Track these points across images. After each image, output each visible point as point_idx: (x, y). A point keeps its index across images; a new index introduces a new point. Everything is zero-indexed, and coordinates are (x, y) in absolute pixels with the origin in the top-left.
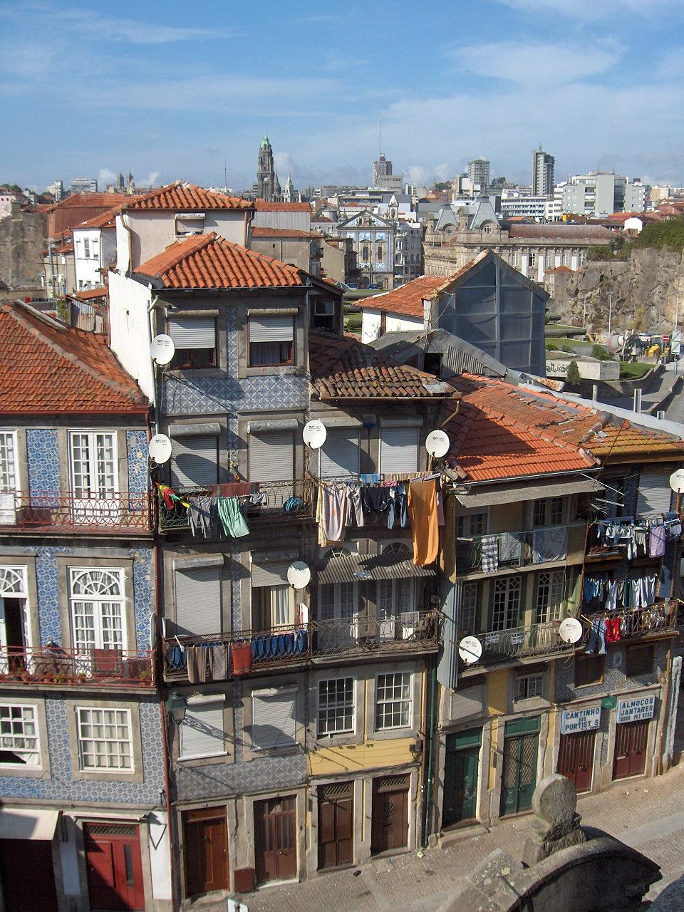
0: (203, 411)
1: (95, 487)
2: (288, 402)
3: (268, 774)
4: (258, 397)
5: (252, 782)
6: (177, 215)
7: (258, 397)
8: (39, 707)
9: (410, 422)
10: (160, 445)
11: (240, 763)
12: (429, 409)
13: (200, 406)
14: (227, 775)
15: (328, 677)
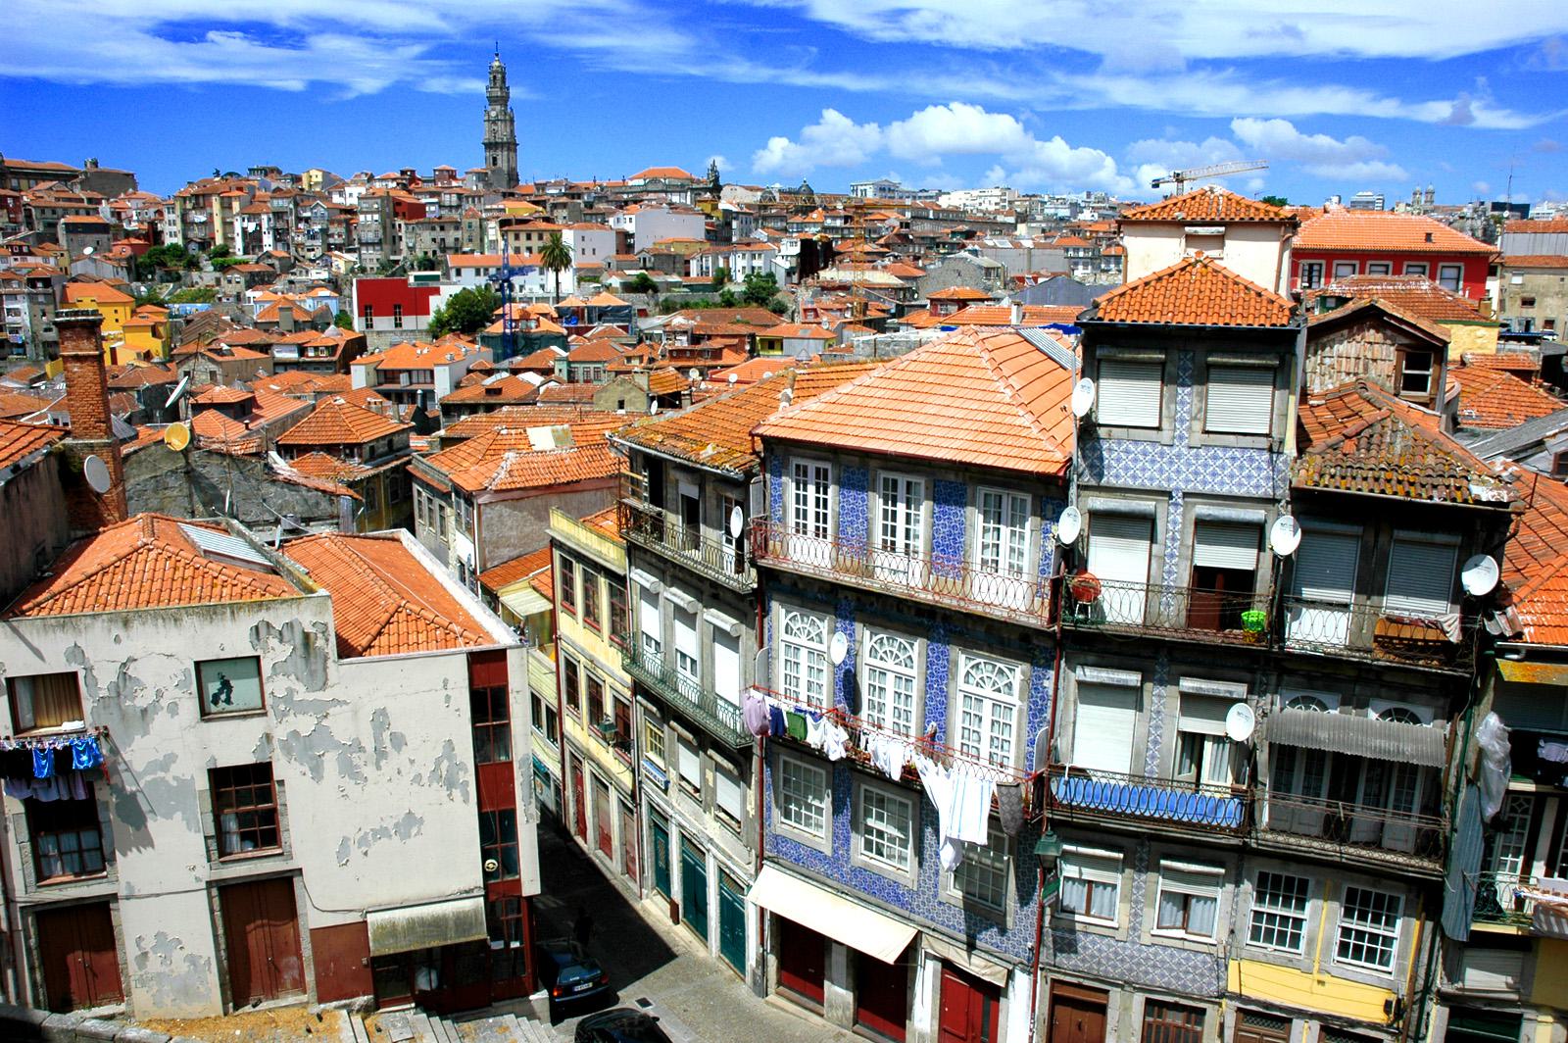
0: (1137, 485)
1: (1004, 561)
2: (1257, 487)
3: (1171, 970)
4: (1214, 474)
5: (1146, 973)
6: (1187, 229)
7: (1214, 474)
8: (914, 804)
9: (1440, 538)
10: (1071, 519)
11: (1134, 943)
12: (1478, 523)
13: (1134, 477)
14: (1116, 953)
15: (1273, 869)
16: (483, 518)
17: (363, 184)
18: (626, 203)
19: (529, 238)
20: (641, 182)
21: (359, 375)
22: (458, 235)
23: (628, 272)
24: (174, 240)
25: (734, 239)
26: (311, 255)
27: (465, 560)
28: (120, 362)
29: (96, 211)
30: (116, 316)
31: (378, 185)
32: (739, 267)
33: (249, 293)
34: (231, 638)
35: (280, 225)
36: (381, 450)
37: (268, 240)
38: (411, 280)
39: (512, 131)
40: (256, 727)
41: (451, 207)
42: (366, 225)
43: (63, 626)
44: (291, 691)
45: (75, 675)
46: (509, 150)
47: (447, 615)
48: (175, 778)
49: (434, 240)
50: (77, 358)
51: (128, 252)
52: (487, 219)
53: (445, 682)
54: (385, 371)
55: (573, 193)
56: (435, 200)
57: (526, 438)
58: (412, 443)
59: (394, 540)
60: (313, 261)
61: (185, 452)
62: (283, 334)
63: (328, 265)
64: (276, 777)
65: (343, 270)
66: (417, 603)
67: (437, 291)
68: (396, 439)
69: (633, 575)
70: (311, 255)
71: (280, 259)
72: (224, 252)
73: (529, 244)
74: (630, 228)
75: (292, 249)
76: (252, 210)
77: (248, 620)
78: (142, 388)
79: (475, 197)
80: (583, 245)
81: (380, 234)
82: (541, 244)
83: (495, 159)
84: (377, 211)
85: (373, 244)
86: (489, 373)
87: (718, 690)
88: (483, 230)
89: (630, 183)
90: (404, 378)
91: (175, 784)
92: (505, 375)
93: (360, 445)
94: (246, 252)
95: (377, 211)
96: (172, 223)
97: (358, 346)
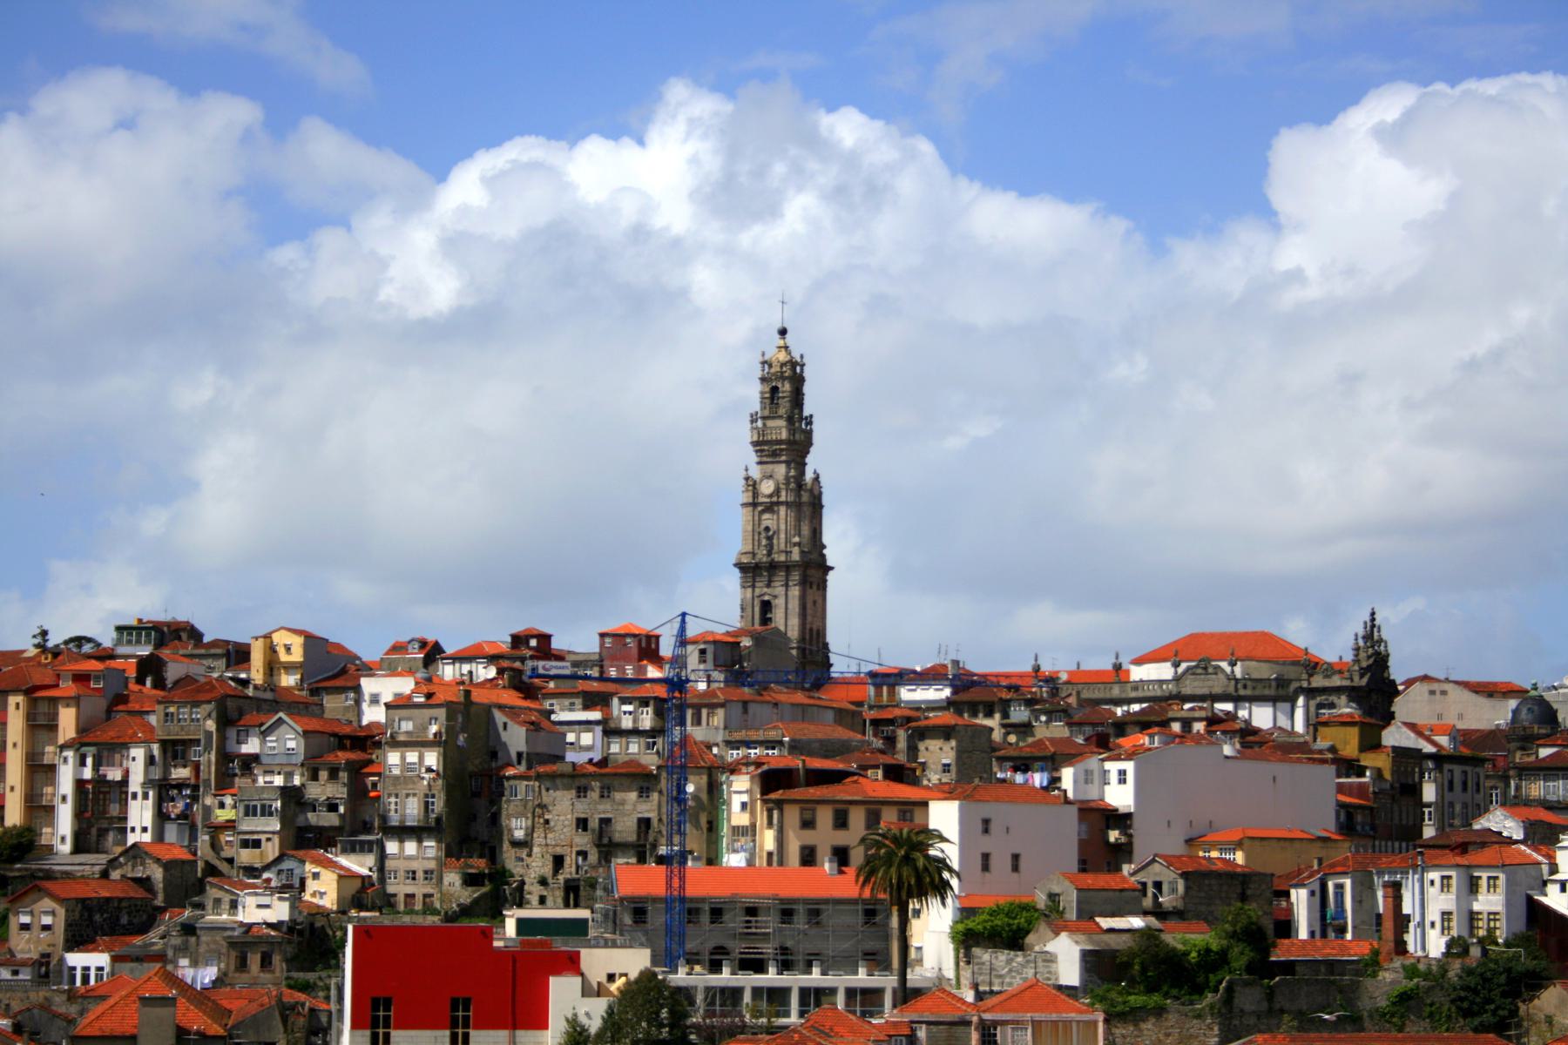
18: (1121, 727)
19: (841, 822)
20: (1164, 671)
22: (649, 808)
23: (1105, 923)
25: (1429, 832)
26: (246, 856)
31: (448, 672)
32: (1433, 914)
33: (76, 959)
35: (181, 773)
37: (141, 814)
38: (510, 928)
39: (816, 533)
41: (635, 732)
46: (805, 583)
49: (582, 824)
52: (733, 770)
55: (973, 693)
56: (595, 715)
60: (252, 871)
63: (293, 889)
65: (329, 902)
67: (571, 964)
70: (246, 856)
71: (168, 866)
73: (842, 838)
74: (1120, 797)
76: (109, 734)
80: (986, 844)
81: (439, 805)
83: (766, 607)
84: (435, 743)
89: (1138, 673)
94: (78, 848)
95: (435, 743)
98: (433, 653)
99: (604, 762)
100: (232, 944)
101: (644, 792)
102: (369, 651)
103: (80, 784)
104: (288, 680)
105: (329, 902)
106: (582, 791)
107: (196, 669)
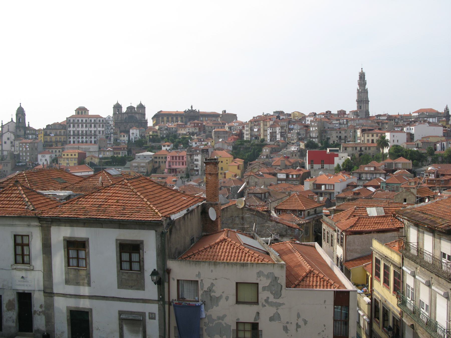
16: (347, 240)
17: (312, 116)
19: (373, 136)
21: (308, 185)
24: (248, 136)
26: (292, 142)
27: (339, 256)
28: (227, 177)
29: (224, 127)
30: (227, 162)
34: (250, 275)
35: (284, 131)
36: (312, 213)
37: (278, 136)
38: (328, 151)
40: (254, 309)
42: (313, 131)
43: (196, 264)
44: (268, 298)
45: (198, 281)
47: (328, 275)
48: (225, 323)
49: (337, 137)
50: (210, 174)
51: (233, 141)
53: (325, 301)
54: (317, 184)
57: (366, 212)
58: (324, 211)
59: (312, 246)
60: (293, 144)
61: (242, 208)
62: (281, 170)
64: (260, 329)
66: (318, 270)
67: (337, 156)
68: (318, 209)
69: (404, 268)
72: (263, 140)
73: (373, 138)
75: (287, 139)
77: (256, 270)
78: (232, 186)
79: (353, 120)
81: (317, 134)
82: (377, 138)
83: (360, 106)
85: (315, 138)
86: (356, 186)
87: (437, 320)
88: (355, 132)
90: (323, 187)
91: (225, 325)
92: (361, 187)
93: (304, 210)
94: (271, 141)
96: (247, 131)
97: (308, 175)
98: (315, 114)
99: (339, 129)
100: (291, 153)
101: (345, 132)
102: (307, 114)
103: (270, 133)
104: (296, 118)
105: (304, 148)
106: (337, 132)
107: (284, 117)
